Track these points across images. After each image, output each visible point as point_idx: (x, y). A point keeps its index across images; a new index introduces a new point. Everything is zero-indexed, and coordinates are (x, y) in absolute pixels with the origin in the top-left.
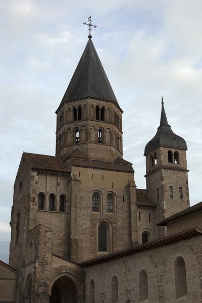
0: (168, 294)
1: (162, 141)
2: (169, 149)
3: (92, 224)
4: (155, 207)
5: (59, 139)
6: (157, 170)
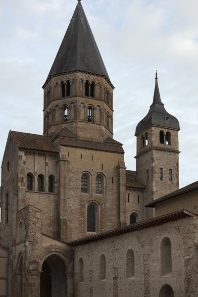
0: (153, 272)
1: (154, 121)
2: (161, 129)
3: (81, 205)
4: (145, 189)
5: (46, 117)
6: (147, 152)
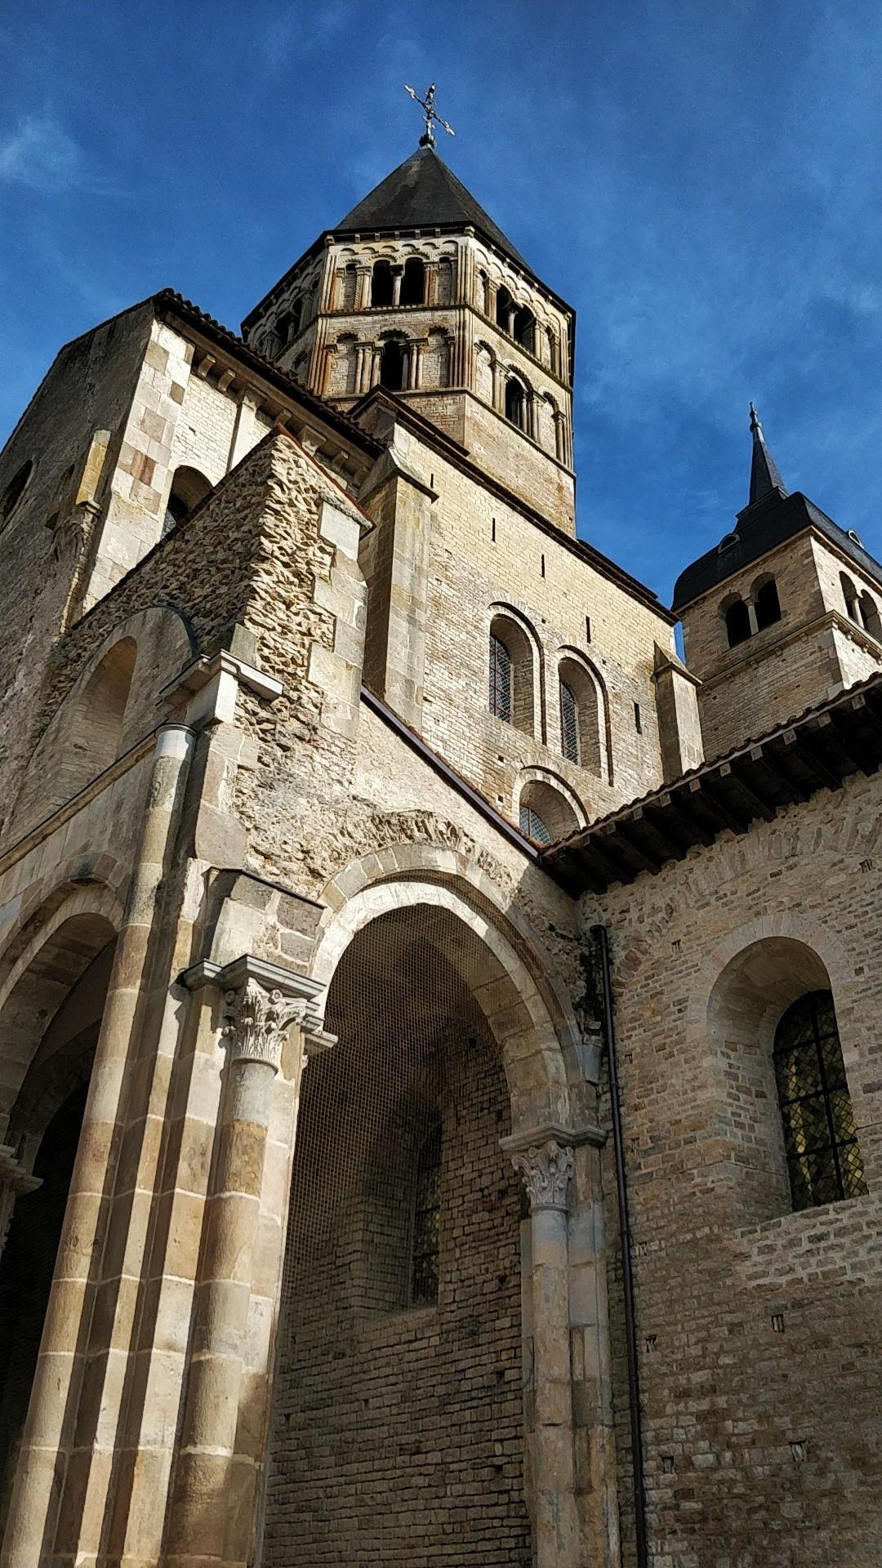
6: (782, 648)
